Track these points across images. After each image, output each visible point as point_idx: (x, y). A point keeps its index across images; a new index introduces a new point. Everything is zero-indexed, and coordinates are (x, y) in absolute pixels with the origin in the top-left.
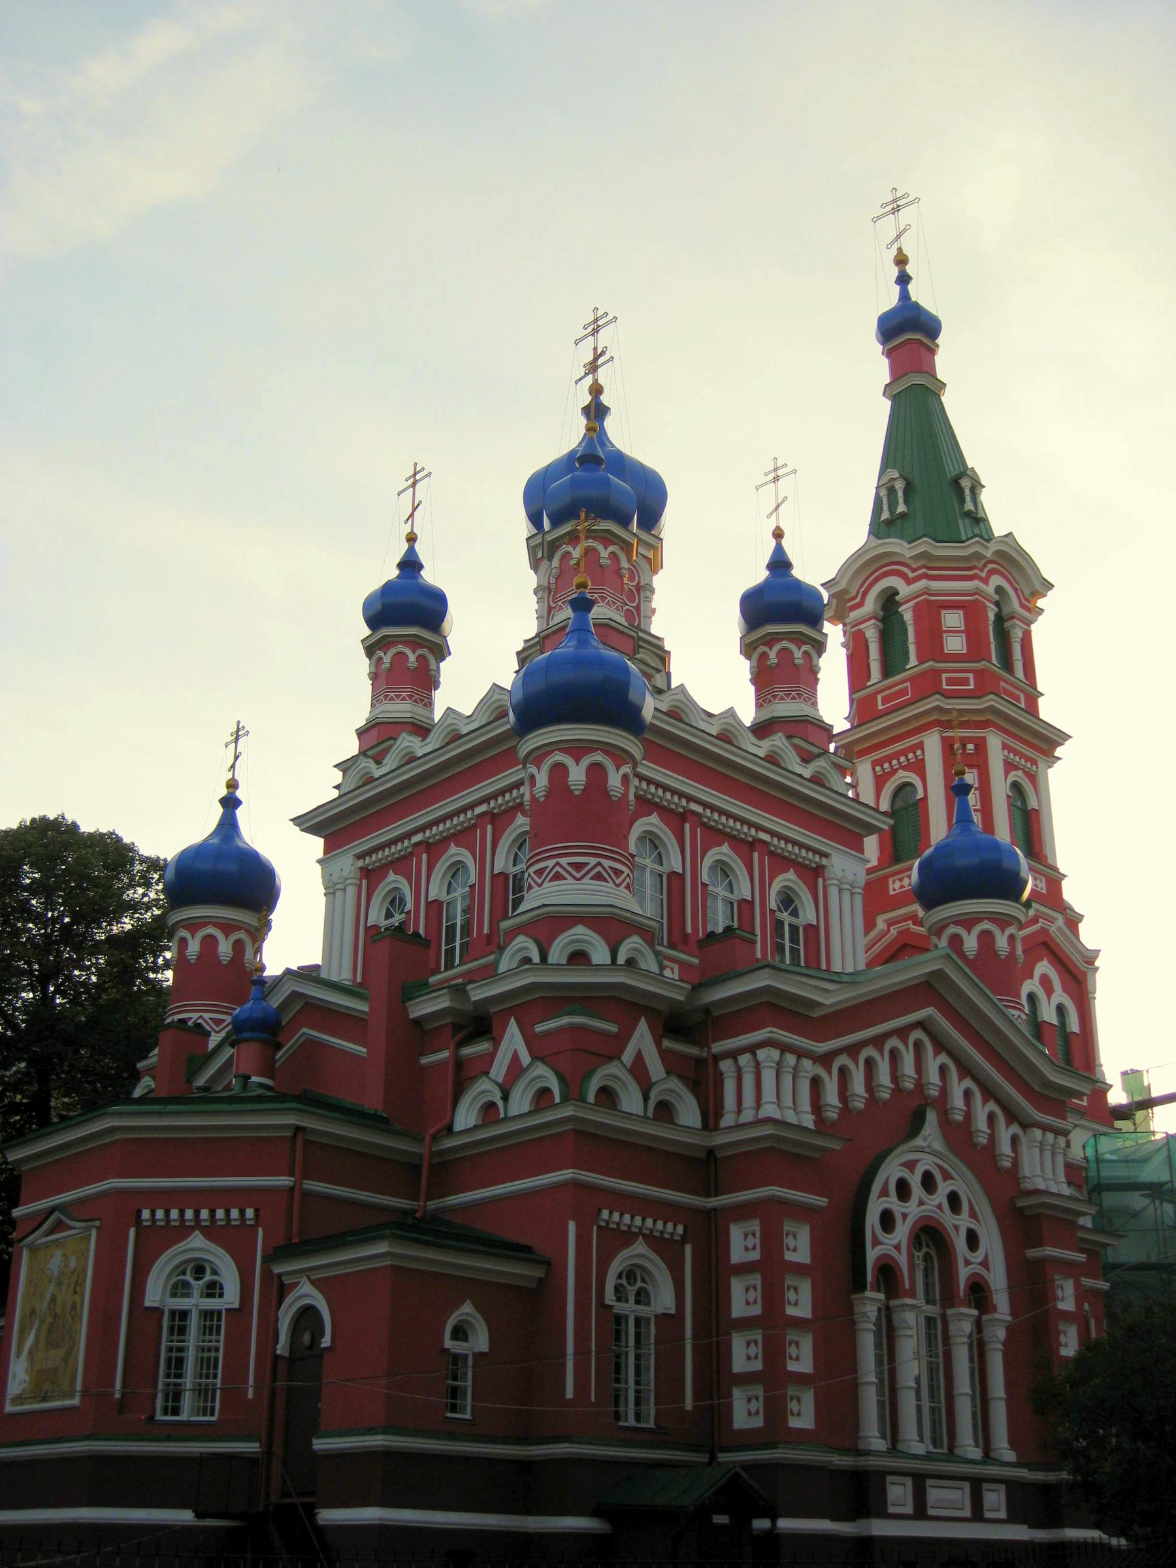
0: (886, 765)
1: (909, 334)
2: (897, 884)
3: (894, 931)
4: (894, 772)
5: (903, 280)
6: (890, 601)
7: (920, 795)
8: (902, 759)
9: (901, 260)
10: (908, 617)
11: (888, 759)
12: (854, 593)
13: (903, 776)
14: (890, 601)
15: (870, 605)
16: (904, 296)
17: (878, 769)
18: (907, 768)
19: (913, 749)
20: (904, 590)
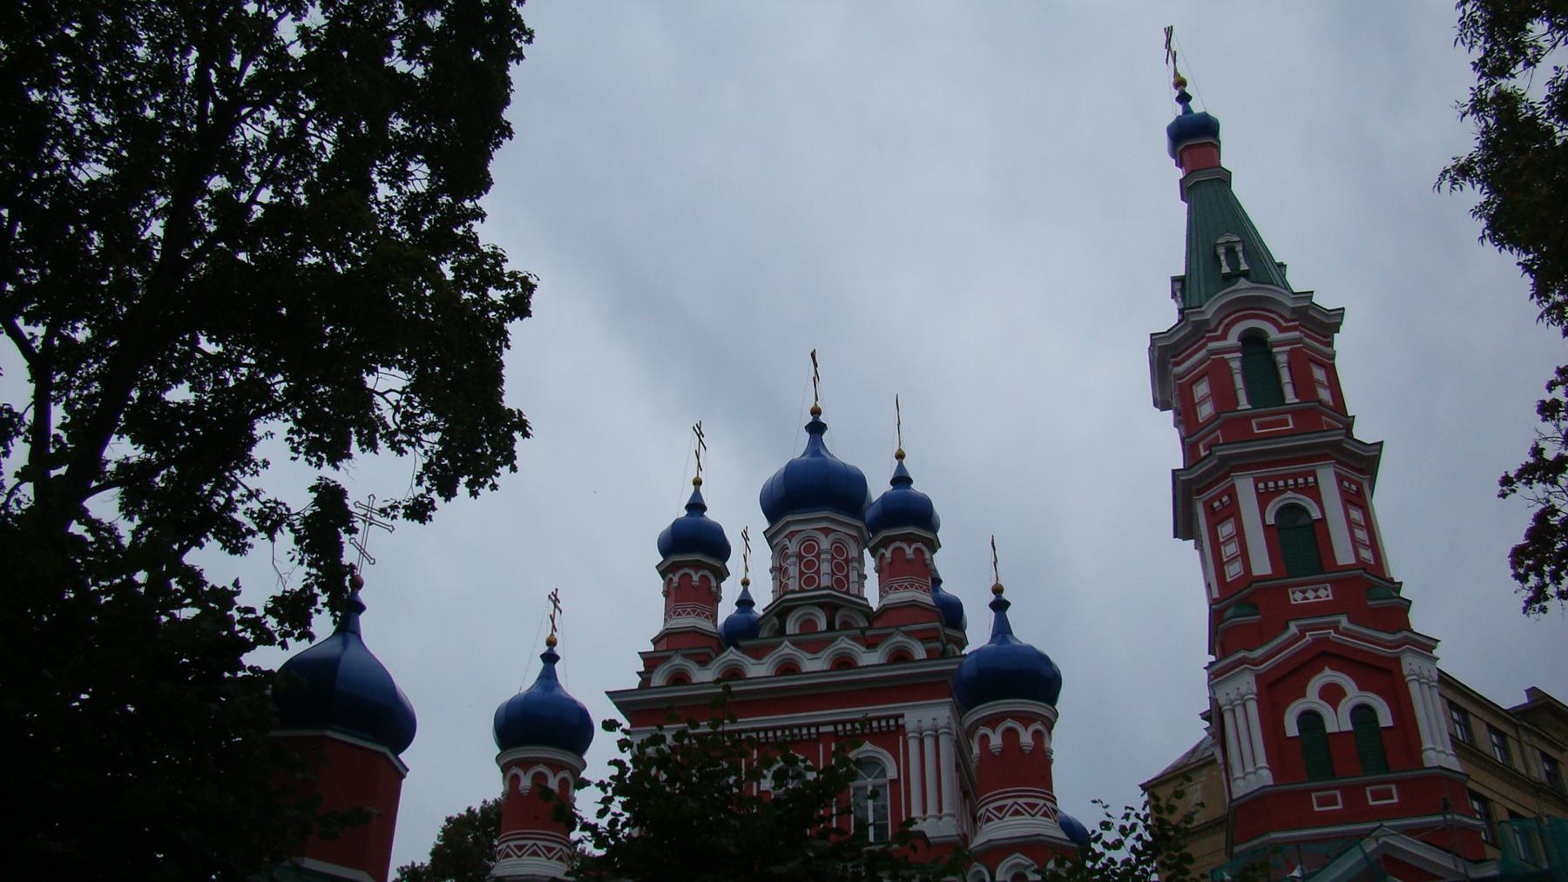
0: (1271, 484)
1: (1194, 138)
2: (1299, 596)
3: (1308, 637)
4: (1278, 492)
5: (1184, 98)
6: (1254, 343)
7: (1316, 514)
8: (1301, 480)
9: (1180, 83)
10: (1282, 359)
11: (1275, 479)
12: (1213, 326)
13: (1290, 497)
14: (1254, 343)
15: (1233, 339)
16: (1187, 110)
17: (1261, 486)
18: (1296, 489)
19: (1305, 475)
20: (1273, 334)
